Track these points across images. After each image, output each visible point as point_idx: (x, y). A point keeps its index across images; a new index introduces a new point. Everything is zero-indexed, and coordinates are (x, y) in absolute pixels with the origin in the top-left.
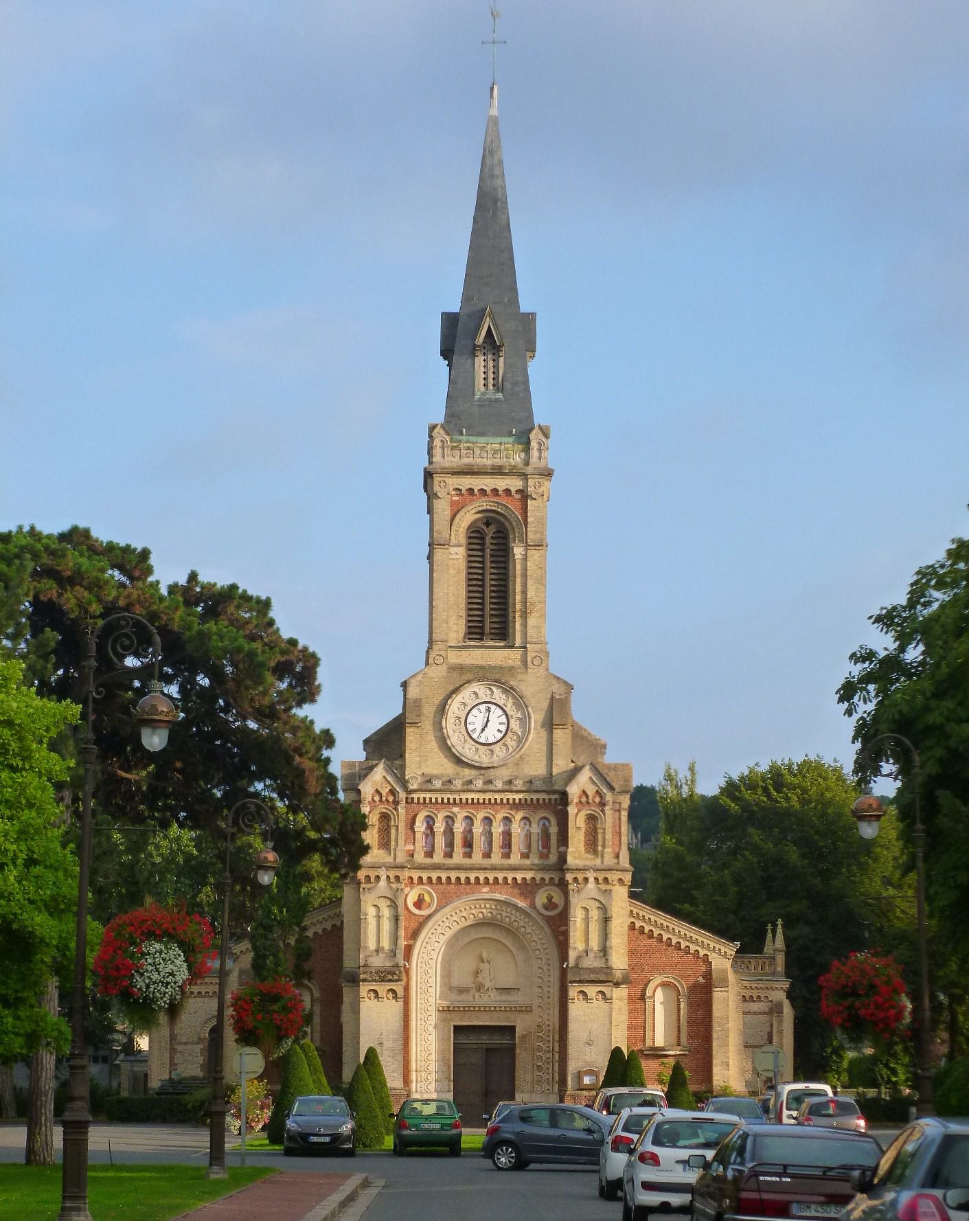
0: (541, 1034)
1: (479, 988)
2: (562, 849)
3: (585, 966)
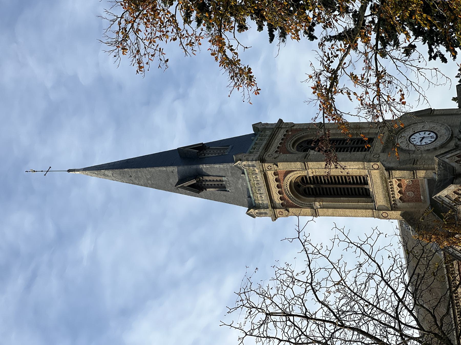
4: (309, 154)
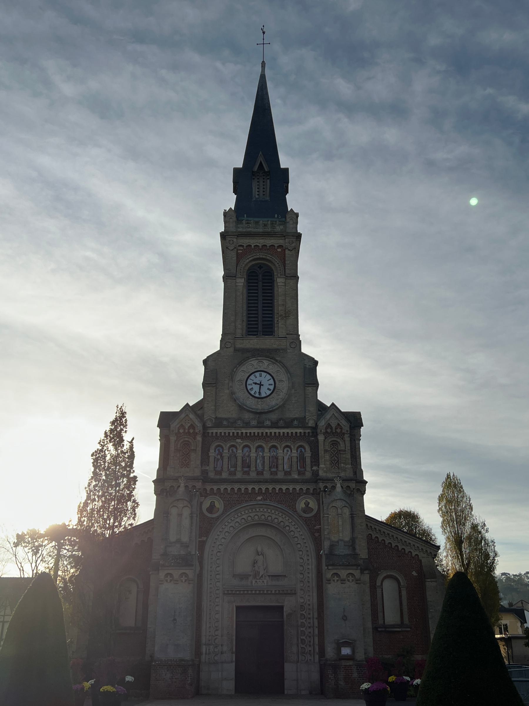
0: (303, 612)
2: (315, 468)
3: (336, 553)
4: (235, 278)
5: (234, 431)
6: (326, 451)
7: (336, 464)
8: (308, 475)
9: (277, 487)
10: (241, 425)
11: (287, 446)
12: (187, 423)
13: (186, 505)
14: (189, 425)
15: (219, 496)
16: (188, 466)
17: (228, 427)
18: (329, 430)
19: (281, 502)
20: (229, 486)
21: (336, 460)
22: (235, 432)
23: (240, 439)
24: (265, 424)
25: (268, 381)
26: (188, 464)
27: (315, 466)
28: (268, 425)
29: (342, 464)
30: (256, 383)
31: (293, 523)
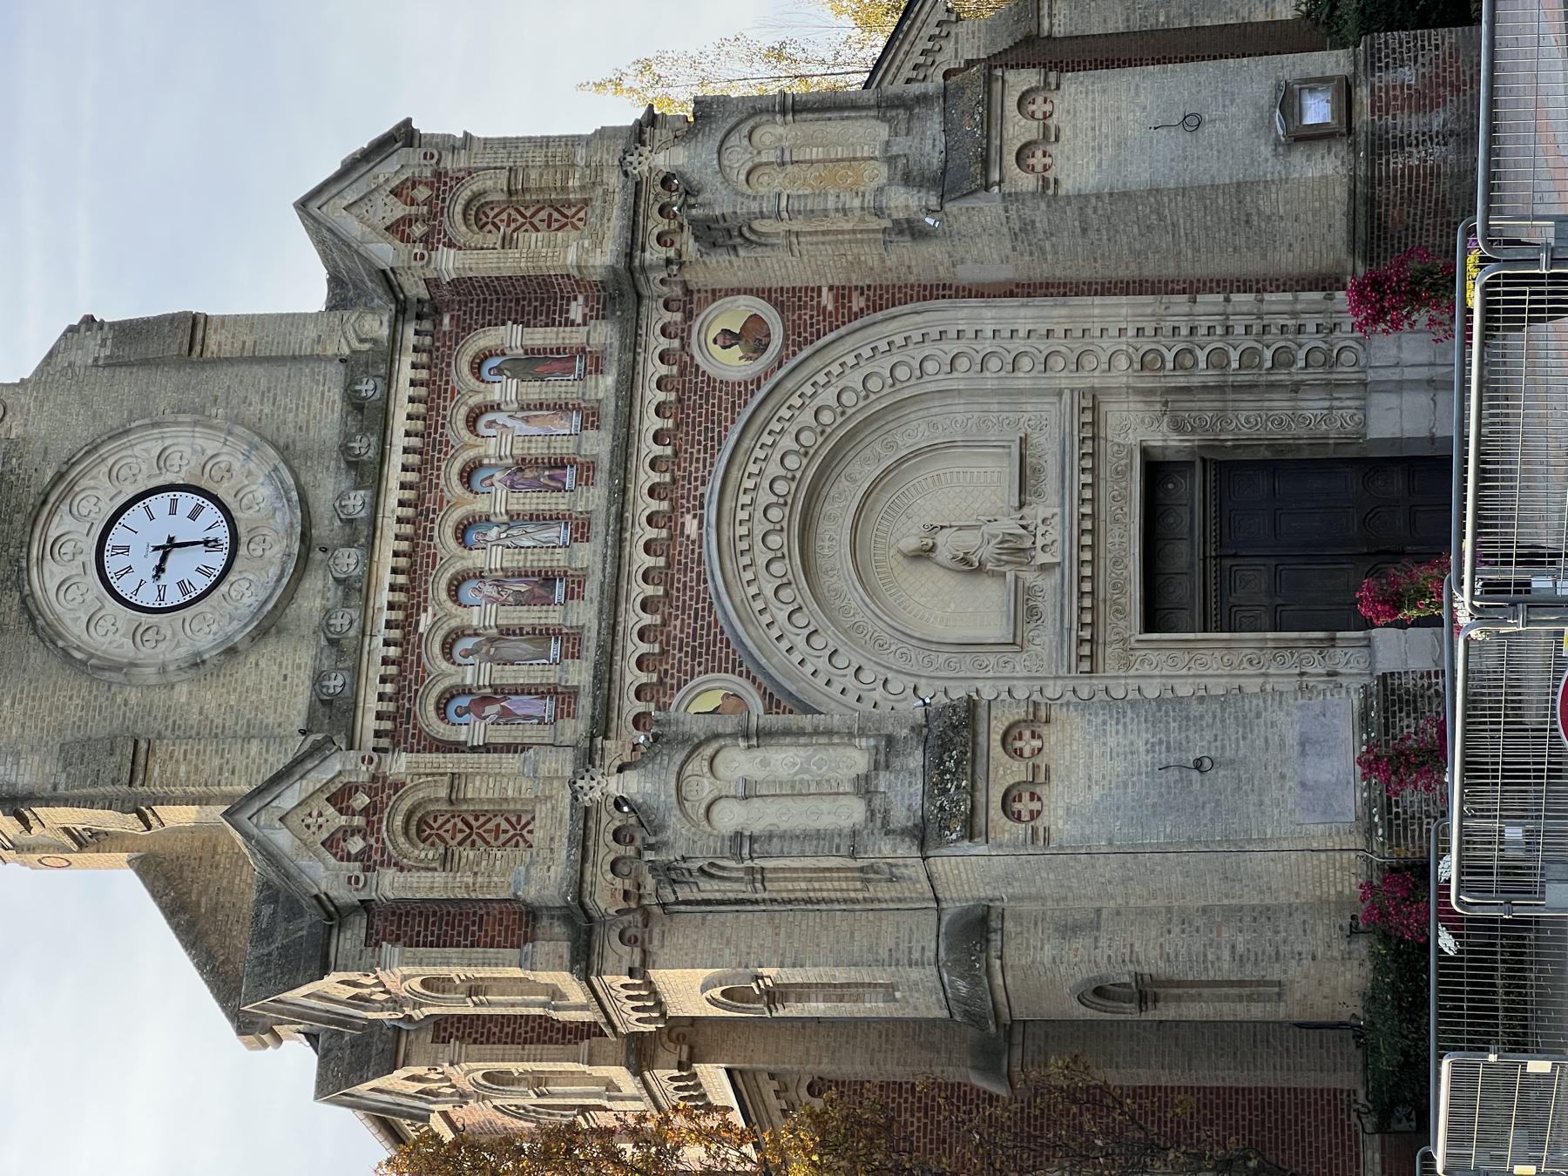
0: (1169, 356)
1: (1016, 551)
3: (936, 161)
5: (379, 641)
6: (507, 242)
7: (567, 217)
8: (604, 335)
9: (649, 448)
10: (355, 614)
11: (472, 421)
12: (320, 820)
13: (706, 763)
14: (332, 809)
15: (672, 696)
16: (523, 822)
17: (356, 672)
18: (418, 230)
19: (712, 439)
20: (630, 647)
21: (550, 215)
22: (385, 596)
23: (418, 615)
24: (363, 514)
25: (152, 518)
26: (514, 820)
27: (568, 311)
28: (367, 500)
29: (570, 183)
30: (160, 569)
31: (808, 390)
